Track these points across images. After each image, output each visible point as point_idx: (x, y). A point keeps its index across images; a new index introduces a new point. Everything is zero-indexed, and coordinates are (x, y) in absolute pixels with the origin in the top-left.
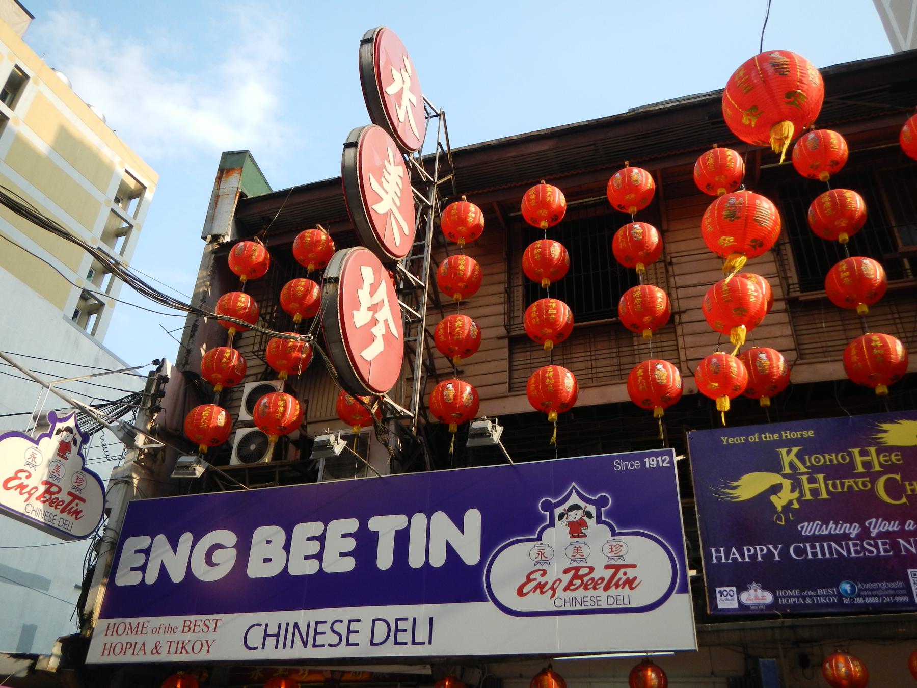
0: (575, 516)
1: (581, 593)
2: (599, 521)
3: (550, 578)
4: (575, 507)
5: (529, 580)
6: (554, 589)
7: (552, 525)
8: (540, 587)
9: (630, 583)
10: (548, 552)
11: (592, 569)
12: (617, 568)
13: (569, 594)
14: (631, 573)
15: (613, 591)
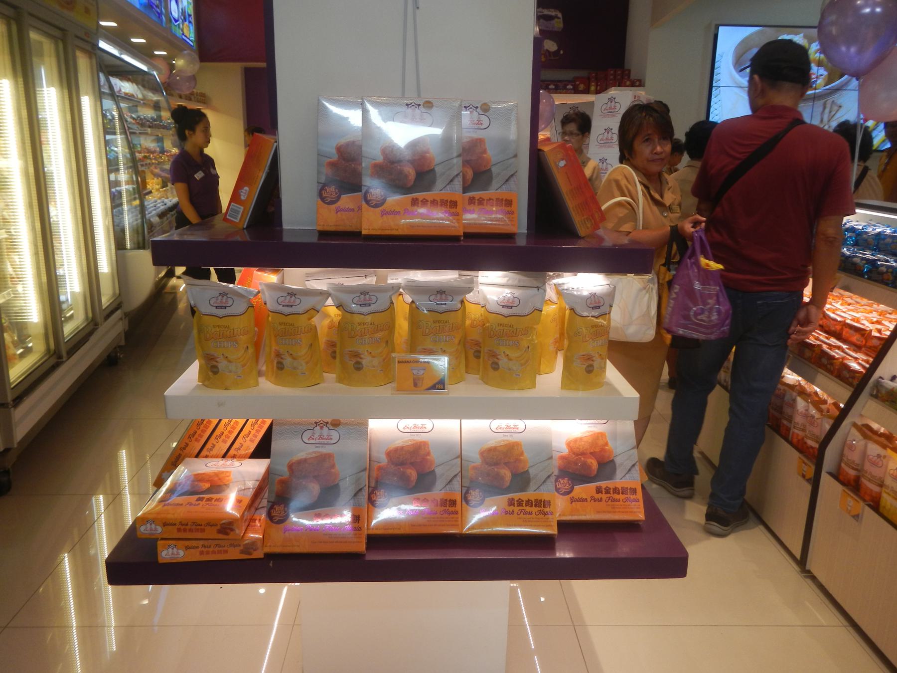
0: (321, 425)
1: (321, 440)
2: (326, 426)
3: (315, 437)
4: (321, 423)
5: (311, 437)
6: (316, 439)
7: (316, 427)
8: (313, 439)
9: (331, 439)
10: (315, 432)
11: (324, 436)
12: (329, 436)
13: (318, 441)
14: (332, 437)
15: (327, 440)
